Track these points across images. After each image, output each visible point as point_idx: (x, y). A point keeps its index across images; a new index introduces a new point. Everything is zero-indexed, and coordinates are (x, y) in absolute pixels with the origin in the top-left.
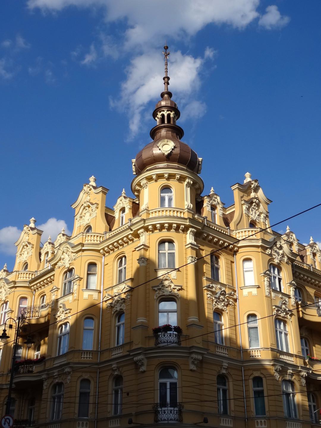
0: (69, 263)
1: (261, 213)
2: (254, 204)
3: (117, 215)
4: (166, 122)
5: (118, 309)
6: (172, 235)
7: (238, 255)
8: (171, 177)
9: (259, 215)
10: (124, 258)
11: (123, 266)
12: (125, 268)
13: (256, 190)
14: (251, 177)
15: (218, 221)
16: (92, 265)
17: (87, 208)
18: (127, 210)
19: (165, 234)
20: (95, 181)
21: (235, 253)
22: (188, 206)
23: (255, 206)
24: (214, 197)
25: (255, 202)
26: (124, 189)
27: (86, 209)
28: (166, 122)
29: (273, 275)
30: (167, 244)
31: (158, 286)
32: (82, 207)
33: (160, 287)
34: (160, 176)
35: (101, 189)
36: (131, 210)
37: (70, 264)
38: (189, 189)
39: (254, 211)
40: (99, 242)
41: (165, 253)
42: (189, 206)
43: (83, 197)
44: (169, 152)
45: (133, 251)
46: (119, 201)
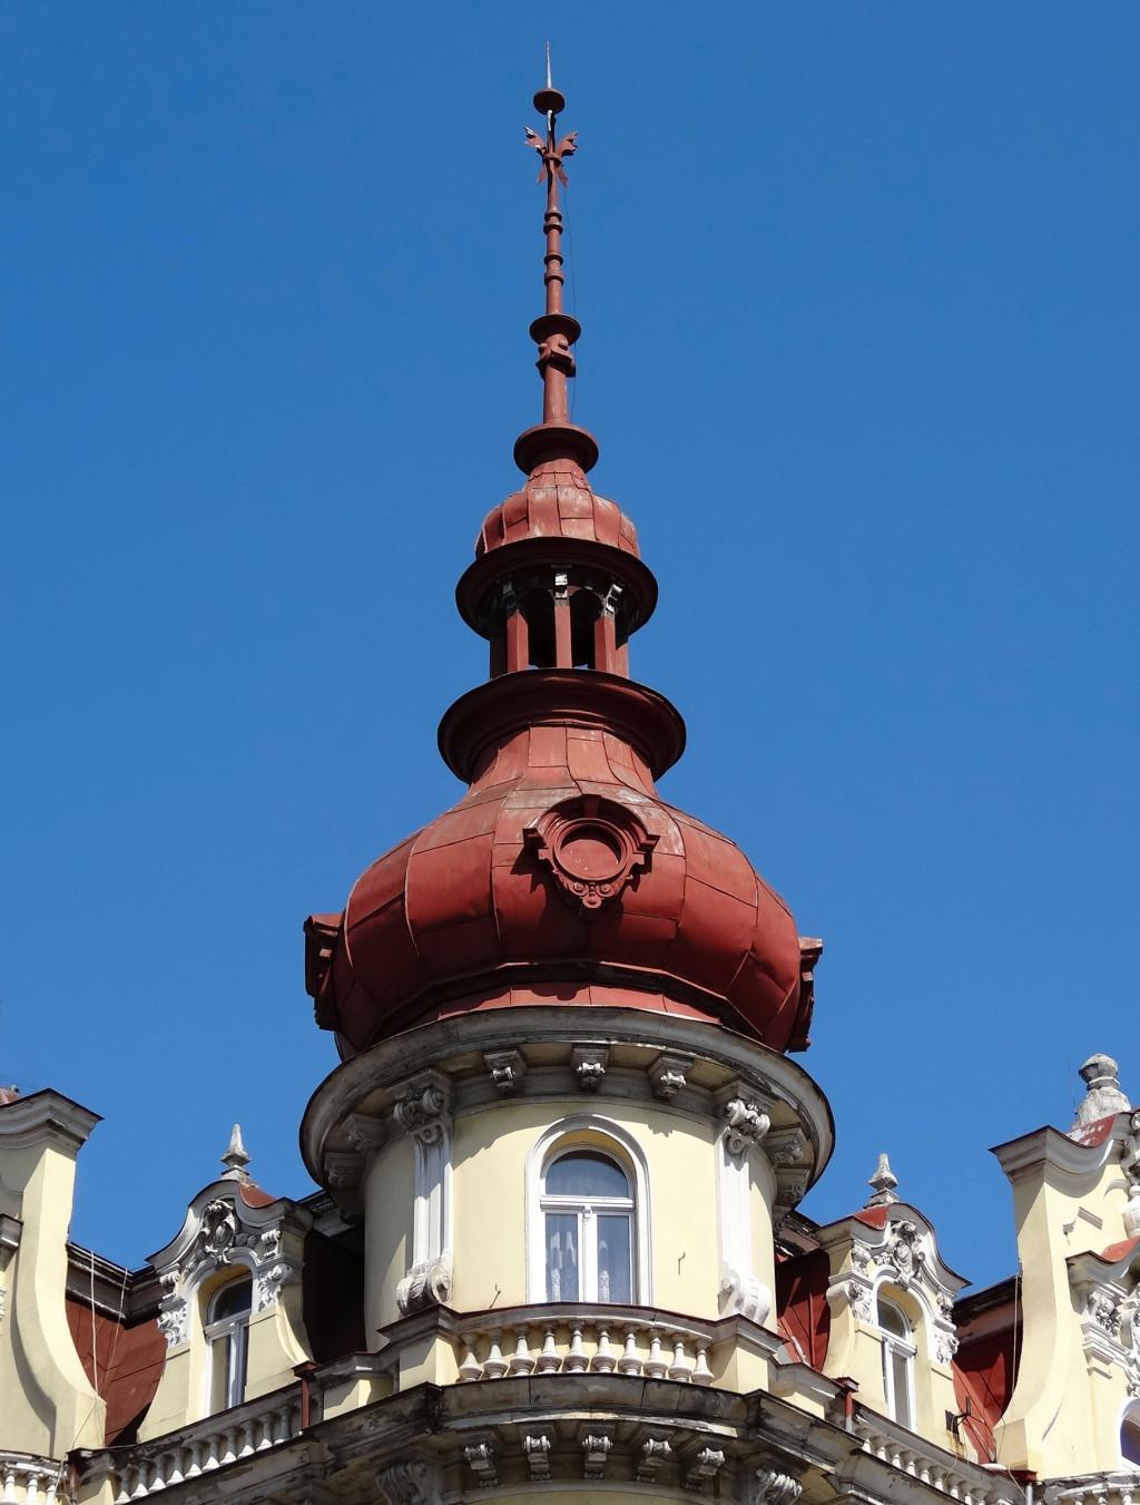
28: (564, 659)
35: (45, 1110)
36: (297, 1294)
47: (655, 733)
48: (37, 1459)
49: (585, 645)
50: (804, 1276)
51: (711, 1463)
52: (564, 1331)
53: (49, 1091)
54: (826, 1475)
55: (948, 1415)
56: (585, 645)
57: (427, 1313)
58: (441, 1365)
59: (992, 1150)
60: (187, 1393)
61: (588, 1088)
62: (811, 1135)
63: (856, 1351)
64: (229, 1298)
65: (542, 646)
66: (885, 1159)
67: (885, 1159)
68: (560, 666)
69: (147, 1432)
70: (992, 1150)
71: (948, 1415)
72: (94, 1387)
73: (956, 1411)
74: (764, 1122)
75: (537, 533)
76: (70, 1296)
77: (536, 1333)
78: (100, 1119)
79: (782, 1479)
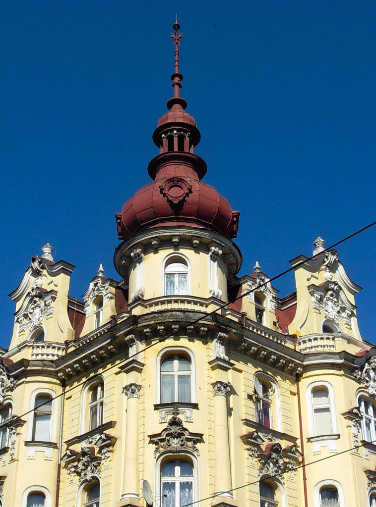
0: (3, 394)
1: (343, 309)
2: (330, 292)
3: (90, 309)
4: (176, 149)
5: (89, 477)
6: (184, 342)
7: (303, 383)
8: (186, 242)
9: (338, 312)
10: (99, 388)
11: (98, 402)
12: (102, 404)
13: (332, 268)
14: (324, 245)
15: (268, 320)
16: (44, 399)
17: (37, 299)
18: (106, 301)
19: (170, 342)
20: (52, 252)
21: (297, 378)
22: (214, 294)
23: (332, 295)
24: (261, 279)
25: (332, 289)
26: (101, 264)
27: (35, 302)
28: (176, 149)
29: (364, 415)
30: (176, 362)
31: (159, 435)
32: (28, 299)
33: (164, 437)
34: (165, 243)
36: (113, 301)
37: (4, 397)
38: (216, 262)
39: (330, 303)
40: (56, 358)
41: (173, 376)
42: (216, 294)
43: (29, 281)
44: (181, 199)
45: (117, 374)
46: (92, 285)
47: (200, 167)
48: (57, 343)
49: (181, 147)
50: (233, 292)
51: (203, 331)
52: (169, 302)
53: (61, 260)
54: (235, 333)
55: (274, 322)
56: (181, 147)
57: (139, 300)
58: (137, 311)
59: (289, 262)
60: (89, 327)
61: (176, 246)
62: (234, 256)
63: (248, 305)
64: (99, 302)
65: (171, 147)
66: (257, 263)
67: (257, 263)
68: (175, 151)
69: (81, 335)
70: (289, 262)
71: (274, 322)
72: (72, 327)
73: (276, 321)
74: (220, 252)
75: (170, 122)
76: (69, 308)
77: (163, 303)
78: (75, 267)
79: (223, 334)
